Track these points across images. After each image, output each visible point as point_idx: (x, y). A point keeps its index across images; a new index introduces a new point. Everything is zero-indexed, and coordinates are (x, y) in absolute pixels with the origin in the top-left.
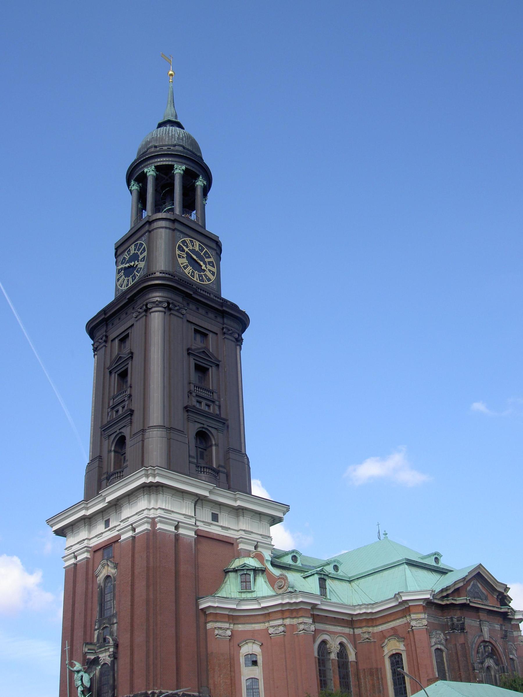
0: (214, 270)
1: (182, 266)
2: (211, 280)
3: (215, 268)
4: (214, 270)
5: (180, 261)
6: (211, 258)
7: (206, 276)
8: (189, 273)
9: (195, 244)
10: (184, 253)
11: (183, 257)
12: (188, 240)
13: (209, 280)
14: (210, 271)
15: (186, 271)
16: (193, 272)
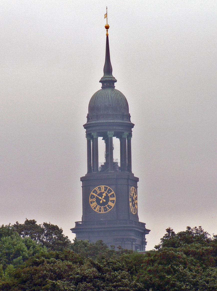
0: (114, 199)
1: (93, 208)
2: (112, 207)
3: (114, 197)
4: (114, 199)
5: (92, 205)
6: (112, 191)
7: (108, 206)
8: (97, 211)
9: (102, 188)
10: (94, 199)
11: (94, 202)
12: (96, 188)
13: (111, 207)
14: (111, 201)
15: (96, 210)
16: (100, 208)
